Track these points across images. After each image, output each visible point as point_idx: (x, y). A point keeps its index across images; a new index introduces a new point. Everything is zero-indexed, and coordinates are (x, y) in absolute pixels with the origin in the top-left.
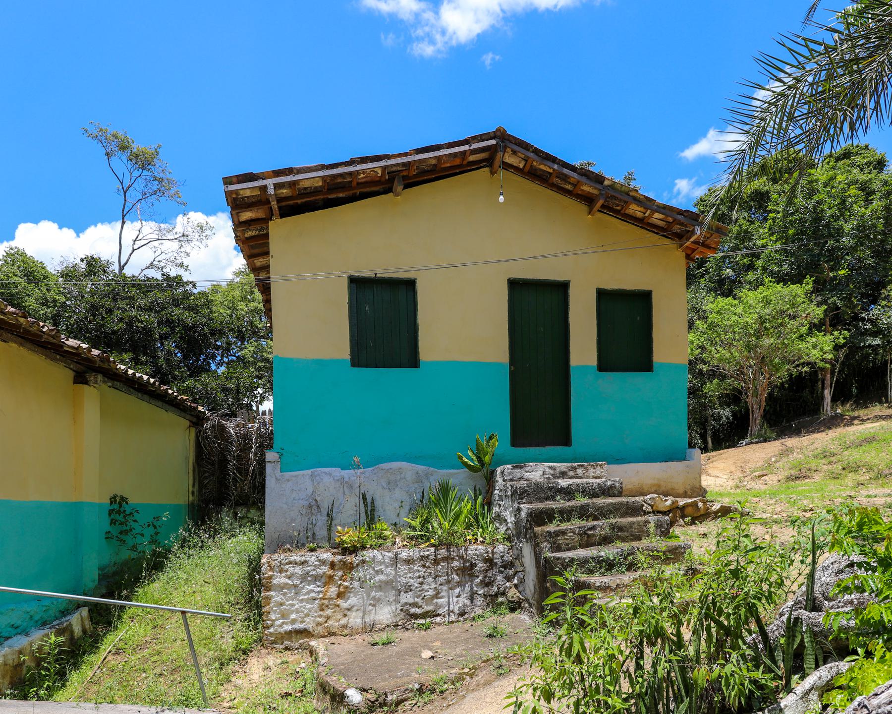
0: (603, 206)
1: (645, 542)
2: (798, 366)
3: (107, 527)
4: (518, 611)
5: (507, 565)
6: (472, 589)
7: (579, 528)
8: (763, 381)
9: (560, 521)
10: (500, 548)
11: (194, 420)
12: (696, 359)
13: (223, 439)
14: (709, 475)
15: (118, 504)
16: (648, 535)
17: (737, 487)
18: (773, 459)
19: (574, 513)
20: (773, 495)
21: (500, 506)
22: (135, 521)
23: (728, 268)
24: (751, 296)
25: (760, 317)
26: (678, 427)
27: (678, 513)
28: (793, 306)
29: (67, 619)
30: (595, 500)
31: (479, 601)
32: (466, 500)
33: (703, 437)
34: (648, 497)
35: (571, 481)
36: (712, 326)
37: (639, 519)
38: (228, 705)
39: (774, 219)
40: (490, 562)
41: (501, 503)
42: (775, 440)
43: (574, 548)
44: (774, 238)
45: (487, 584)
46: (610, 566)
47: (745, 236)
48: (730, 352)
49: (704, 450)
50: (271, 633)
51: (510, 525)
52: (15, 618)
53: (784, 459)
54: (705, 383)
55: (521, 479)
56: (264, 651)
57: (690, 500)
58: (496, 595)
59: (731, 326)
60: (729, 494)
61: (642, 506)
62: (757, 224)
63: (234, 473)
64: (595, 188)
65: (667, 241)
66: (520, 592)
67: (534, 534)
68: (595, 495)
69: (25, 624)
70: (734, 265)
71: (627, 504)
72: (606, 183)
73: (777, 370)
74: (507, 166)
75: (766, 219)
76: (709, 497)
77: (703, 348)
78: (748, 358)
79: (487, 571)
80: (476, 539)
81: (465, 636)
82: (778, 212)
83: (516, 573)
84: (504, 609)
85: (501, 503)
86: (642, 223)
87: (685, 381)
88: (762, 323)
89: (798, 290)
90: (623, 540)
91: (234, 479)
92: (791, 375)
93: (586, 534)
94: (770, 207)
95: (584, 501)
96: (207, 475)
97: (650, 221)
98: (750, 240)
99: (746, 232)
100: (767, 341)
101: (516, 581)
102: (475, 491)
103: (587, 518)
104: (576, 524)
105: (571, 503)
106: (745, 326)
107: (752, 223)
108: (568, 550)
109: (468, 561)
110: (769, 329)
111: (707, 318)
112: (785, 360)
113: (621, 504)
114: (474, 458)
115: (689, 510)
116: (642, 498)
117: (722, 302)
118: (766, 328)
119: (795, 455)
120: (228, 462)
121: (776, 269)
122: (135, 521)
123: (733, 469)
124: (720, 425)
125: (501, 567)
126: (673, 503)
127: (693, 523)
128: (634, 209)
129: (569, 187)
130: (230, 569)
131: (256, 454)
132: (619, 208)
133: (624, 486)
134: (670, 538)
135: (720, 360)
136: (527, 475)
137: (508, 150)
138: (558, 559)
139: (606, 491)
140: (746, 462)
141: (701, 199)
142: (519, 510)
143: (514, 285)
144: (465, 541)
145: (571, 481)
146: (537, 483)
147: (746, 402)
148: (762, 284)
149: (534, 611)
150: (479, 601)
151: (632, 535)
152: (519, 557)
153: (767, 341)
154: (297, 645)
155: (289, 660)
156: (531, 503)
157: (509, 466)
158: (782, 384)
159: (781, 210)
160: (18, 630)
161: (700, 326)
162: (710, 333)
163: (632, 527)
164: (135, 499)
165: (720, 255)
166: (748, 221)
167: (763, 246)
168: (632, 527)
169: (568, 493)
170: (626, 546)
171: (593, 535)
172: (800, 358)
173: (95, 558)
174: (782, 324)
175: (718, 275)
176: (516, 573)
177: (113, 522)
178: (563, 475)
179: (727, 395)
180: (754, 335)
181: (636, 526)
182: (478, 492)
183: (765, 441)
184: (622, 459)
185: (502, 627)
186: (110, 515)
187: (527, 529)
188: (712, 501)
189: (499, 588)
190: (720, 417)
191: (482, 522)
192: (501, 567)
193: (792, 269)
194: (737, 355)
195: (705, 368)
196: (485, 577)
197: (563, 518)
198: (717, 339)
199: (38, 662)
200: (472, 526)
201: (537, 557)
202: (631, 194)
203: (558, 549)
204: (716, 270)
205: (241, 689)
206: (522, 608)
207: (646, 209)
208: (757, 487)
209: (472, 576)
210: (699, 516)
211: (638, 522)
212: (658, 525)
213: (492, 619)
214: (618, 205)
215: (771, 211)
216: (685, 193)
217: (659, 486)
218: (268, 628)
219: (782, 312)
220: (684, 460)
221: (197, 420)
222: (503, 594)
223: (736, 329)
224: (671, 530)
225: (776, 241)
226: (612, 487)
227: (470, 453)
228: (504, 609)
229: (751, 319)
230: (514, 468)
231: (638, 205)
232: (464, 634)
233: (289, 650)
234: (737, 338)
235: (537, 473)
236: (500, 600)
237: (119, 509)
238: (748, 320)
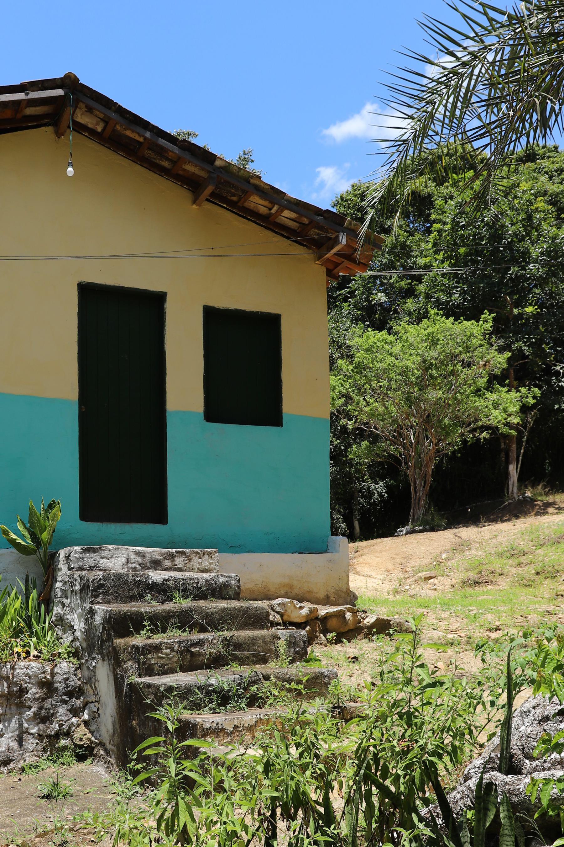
0: (213, 194)
1: (272, 667)
2: (474, 430)
4: (89, 760)
5: (74, 693)
6: (21, 725)
7: (179, 642)
8: (428, 446)
9: (152, 631)
10: (64, 667)
12: (338, 411)
14: (357, 573)
16: (277, 656)
17: (396, 592)
18: (444, 556)
19: (172, 620)
20: (445, 606)
21: (63, 605)
23: (379, 291)
24: (414, 333)
25: (424, 361)
26: (317, 506)
27: (318, 626)
28: (467, 349)
30: (202, 603)
31: (31, 743)
32: (13, 594)
33: (348, 519)
34: (277, 601)
35: (167, 575)
36: (360, 368)
37: (264, 632)
39: (439, 231)
40: (47, 686)
41: (65, 601)
42: (445, 529)
43: (173, 671)
44: (440, 257)
45: (44, 718)
46: (223, 699)
47: (402, 251)
48: (384, 405)
49: (352, 538)
51: (78, 634)
53: (458, 557)
54: (350, 446)
55: (94, 567)
57: (334, 609)
58: (57, 736)
59: (385, 370)
60: (386, 602)
61: (268, 614)
62: (417, 236)
64: (203, 169)
65: (300, 250)
66: (92, 732)
67: (114, 649)
68: (202, 596)
70: (387, 289)
71: (246, 611)
72: (218, 163)
73: (448, 435)
74: (79, 128)
75: (428, 231)
76: (360, 604)
77: (347, 397)
78: (408, 416)
79: (43, 699)
80: (28, 653)
81: (10, 795)
82: (445, 223)
83: (86, 704)
84: (68, 757)
85: (65, 601)
86: (268, 222)
87: (324, 442)
88: (426, 370)
89: (475, 329)
90: (242, 662)
92: (465, 442)
93: (188, 651)
94: (433, 217)
95: (186, 603)
97: (278, 220)
98: (409, 256)
99: (404, 245)
100: (434, 394)
101: (86, 716)
102: (27, 581)
103: (191, 628)
104: (174, 636)
105: (167, 606)
106: (405, 372)
107: (411, 234)
108: (165, 673)
109: (16, 684)
110: (436, 378)
111: (352, 356)
112: (458, 422)
113: (239, 610)
114: (26, 534)
115: (333, 623)
116: (267, 602)
117: (374, 337)
118: (432, 376)
119: (473, 551)
121: (443, 298)
123: (390, 566)
124: (371, 504)
125: (65, 694)
126: (312, 611)
127: (338, 641)
128: (256, 202)
129: (166, 164)
132: (235, 199)
133: (242, 584)
134: (307, 661)
135: (371, 415)
136: (104, 563)
137: (81, 105)
138: (149, 686)
139: (218, 591)
140: (408, 558)
141: (342, 198)
142: (92, 612)
143: (88, 293)
144: (12, 654)
145: (167, 575)
146: (118, 576)
147: (406, 475)
148: (426, 316)
149: (113, 761)
150: (31, 743)
151: (254, 656)
152: (91, 680)
153: (434, 394)
156: (109, 603)
157: (78, 548)
158: (454, 453)
159: (448, 220)
161: (344, 368)
162: (358, 377)
163: (254, 644)
165: (370, 273)
166: (405, 231)
167: (428, 267)
168: (254, 644)
169: (163, 591)
170: (247, 671)
171: (199, 654)
172: (477, 420)
174: (453, 373)
175: (367, 299)
176: (86, 704)
178: (156, 564)
179: (380, 463)
180: (417, 384)
181: (260, 642)
182: (31, 584)
183: (432, 530)
184: (239, 546)
185: (64, 783)
187: (103, 641)
188: (364, 612)
189: (61, 726)
190: (370, 494)
191: (37, 628)
192: (65, 694)
193: (465, 299)
194: (394, 410)
195: (351, 425)
196: (41, 708)
197: (156, 626)
198: (367, 386)
200: (22, 633)
201: (118, 682)
202: (252, 181)
203: (150, 671)
204: (363, 293)
206: (95, 756)
207: (273, 203)
208: (423, 593)
209: (22, 706)
210: (347, 632)
211: (264, 638)
212: (291, 643)
213: (51, 772)
214: (234, 195)
215: (435, 221)
216: (324, 187)
217: (291, 587)
219: (454, 357)
220: (326, 552)
222: (68, 734)
223: (392, 375)
224: (309, 649)
225: (443, 262)
226: (226, 586)
227: (20, 527)
228: (68, 757)
229: (411, 362)
230: (84, 551)
231: (261, 197)
232: (9, 793)
234: (394, 386)
235: (117, 560)
236: (62, 742)
238: (409, 363)
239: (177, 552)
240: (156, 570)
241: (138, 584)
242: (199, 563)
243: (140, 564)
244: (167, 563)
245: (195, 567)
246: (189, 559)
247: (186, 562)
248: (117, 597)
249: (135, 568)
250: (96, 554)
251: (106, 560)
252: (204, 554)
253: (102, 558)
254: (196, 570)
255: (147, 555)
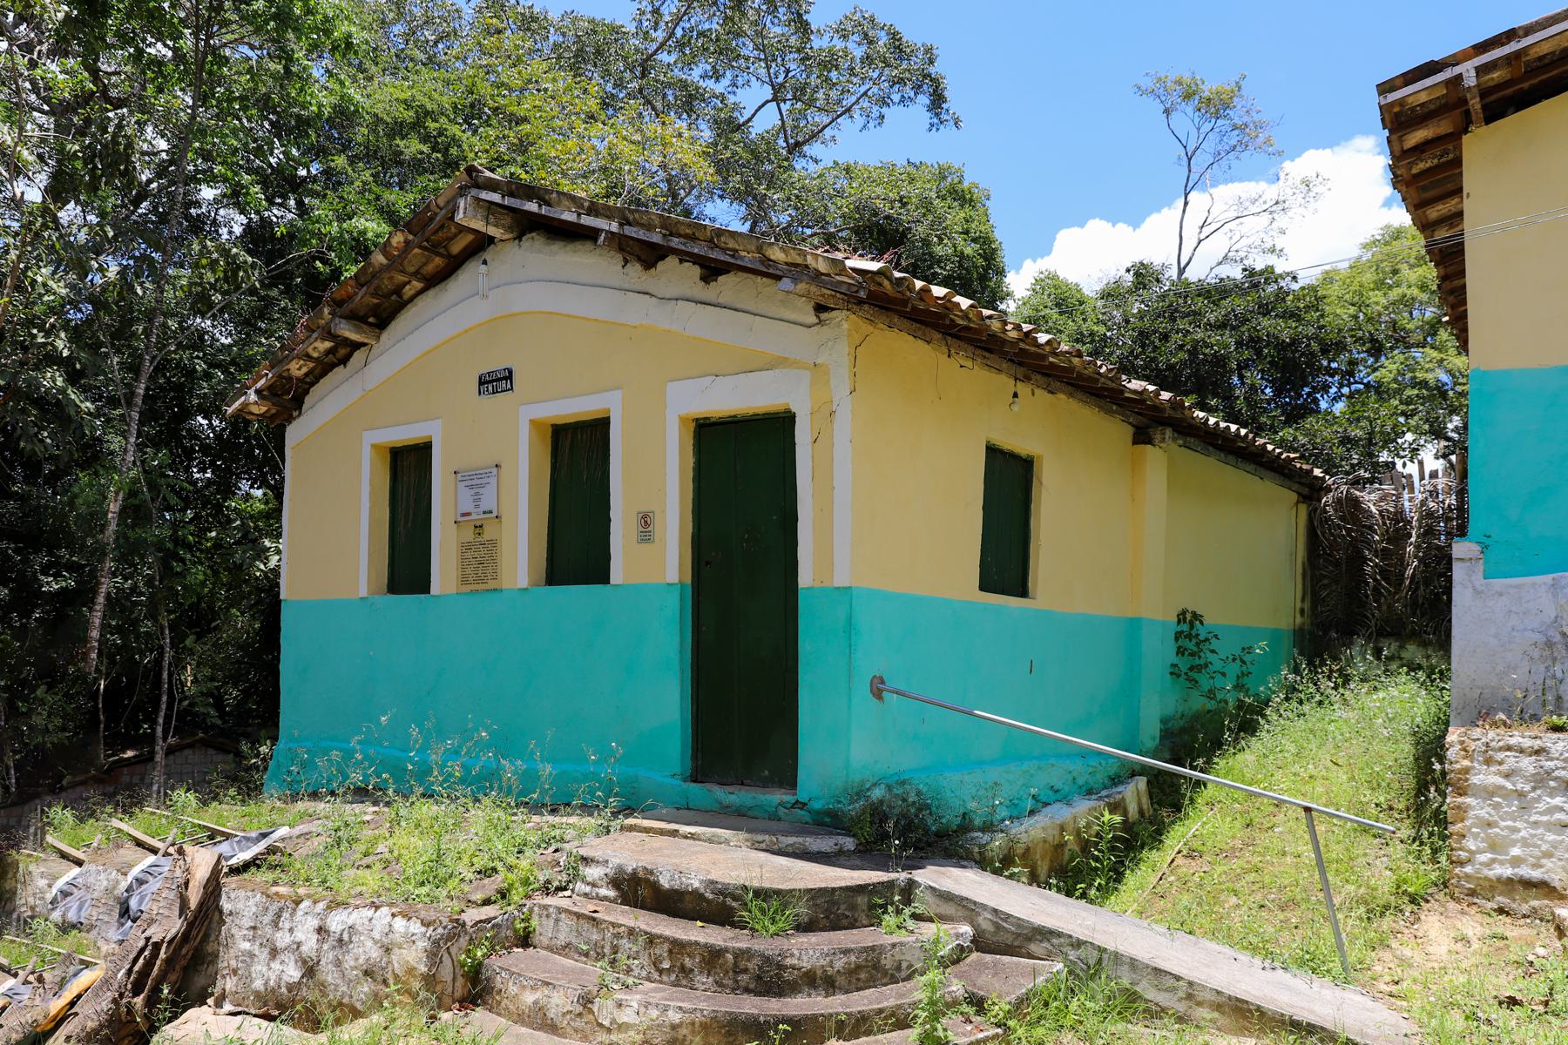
3: (1174, 659)
11: (1306, 491)
13: (1355, 520)
15: (1189, 621)
22: (1213, 651)
29: (1120, 788)
38: (1388, 989)
50: (1467, 876)
52: (1056, 777)
56: (1452, 905)
63: (1375, 580)
69: (1066, 788)
91: (1376, 590)
96: (1326, 581)
120: (1364, 560)
122: (1213, 651)
130: (1376, 746)
131: (1418, 547)
154: (1525, 908)
155: (1508, 934)
160: (1058, 796)
164: (1213, 618)
173: (1157, 703)
177: (1180, 651)
186: (1177, 639)
199: (1085, 846)
205: (1411, 966)
218: (1462, 864)
221: (1310, 491)
233: (1508, 914)
237: (1189, 631)
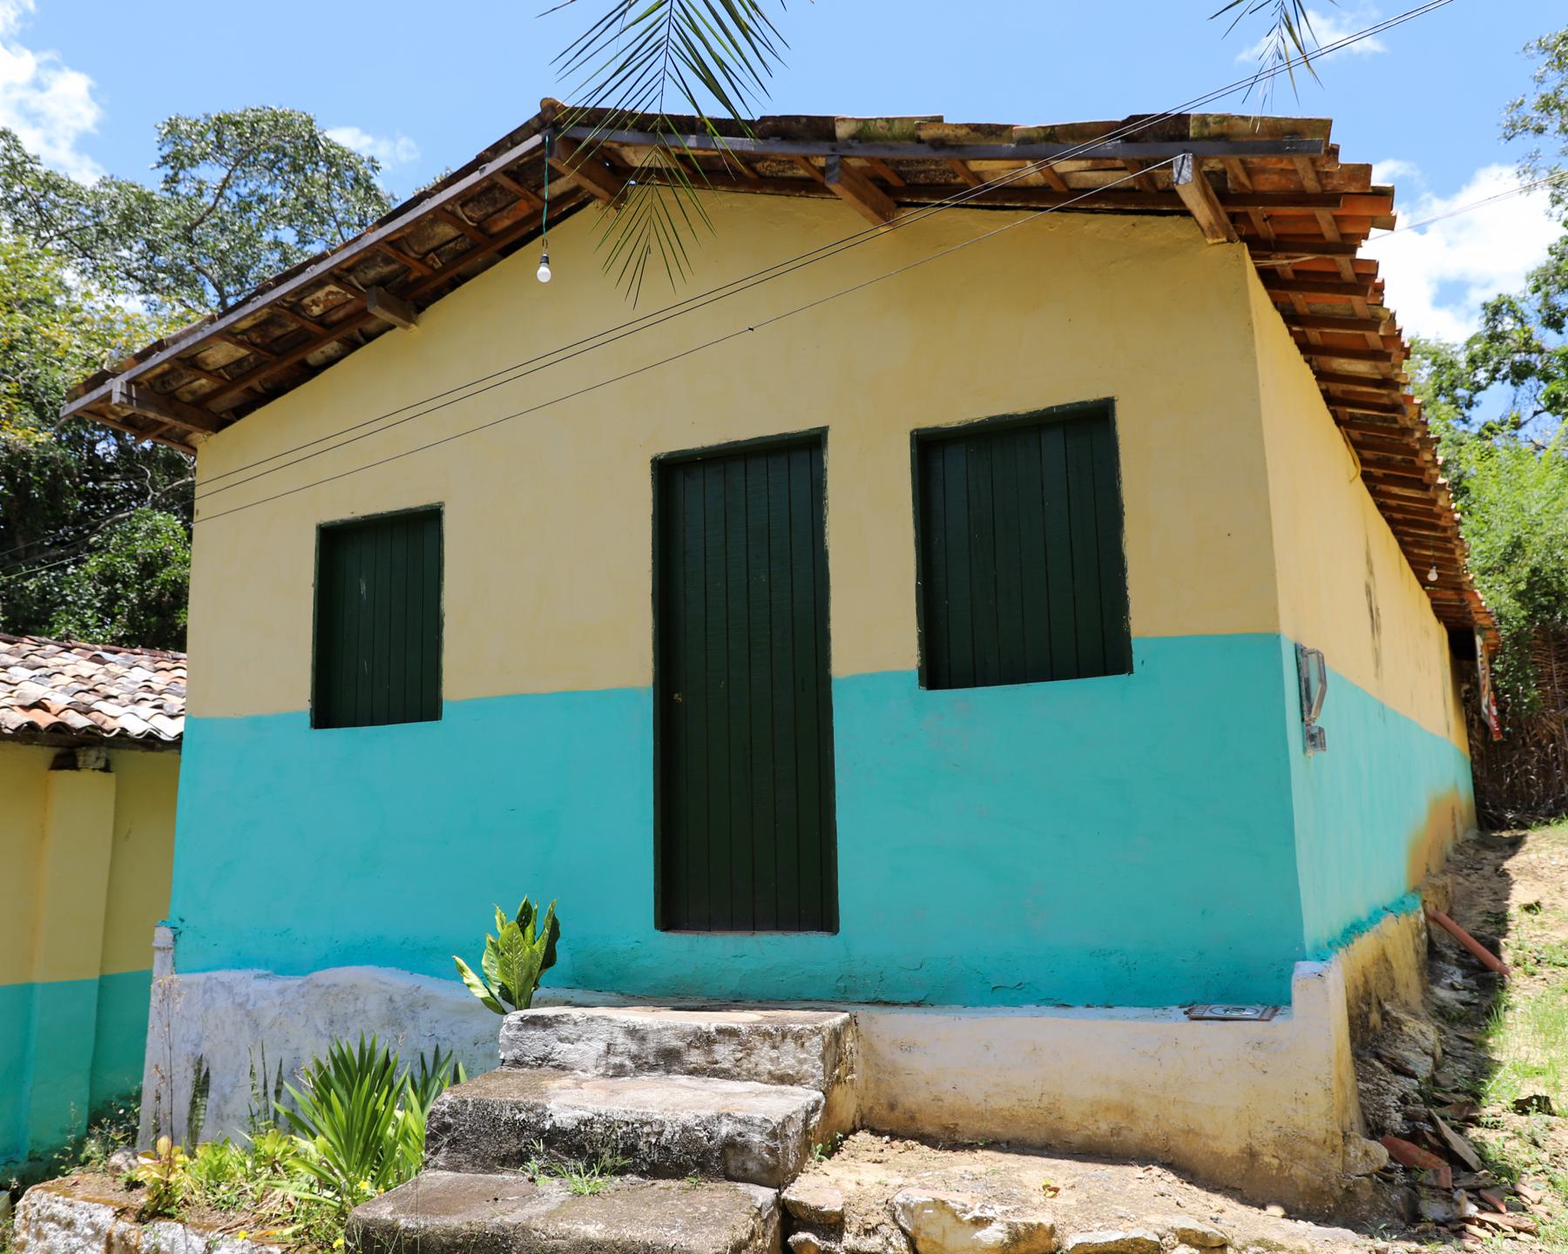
239: (720, 1031)
240: (668, 1072)
241: (520, 1128)
242: (771, 1060)
243: (634, 1058)
244: (695, 1057)
245: (761, 1068)
246: (748, 1050)
247: (740, 1055)
248: (475, 1157)
249: (622, 1066)
250: (549, 1031)
251: (568, 1046)
252: (784, 1037)
253: (560, 1040)
254: (765, 1077)
255: (651, 1036)
